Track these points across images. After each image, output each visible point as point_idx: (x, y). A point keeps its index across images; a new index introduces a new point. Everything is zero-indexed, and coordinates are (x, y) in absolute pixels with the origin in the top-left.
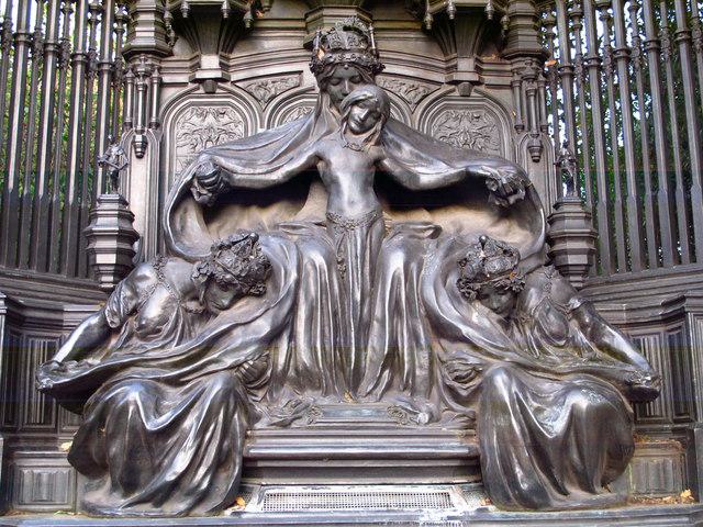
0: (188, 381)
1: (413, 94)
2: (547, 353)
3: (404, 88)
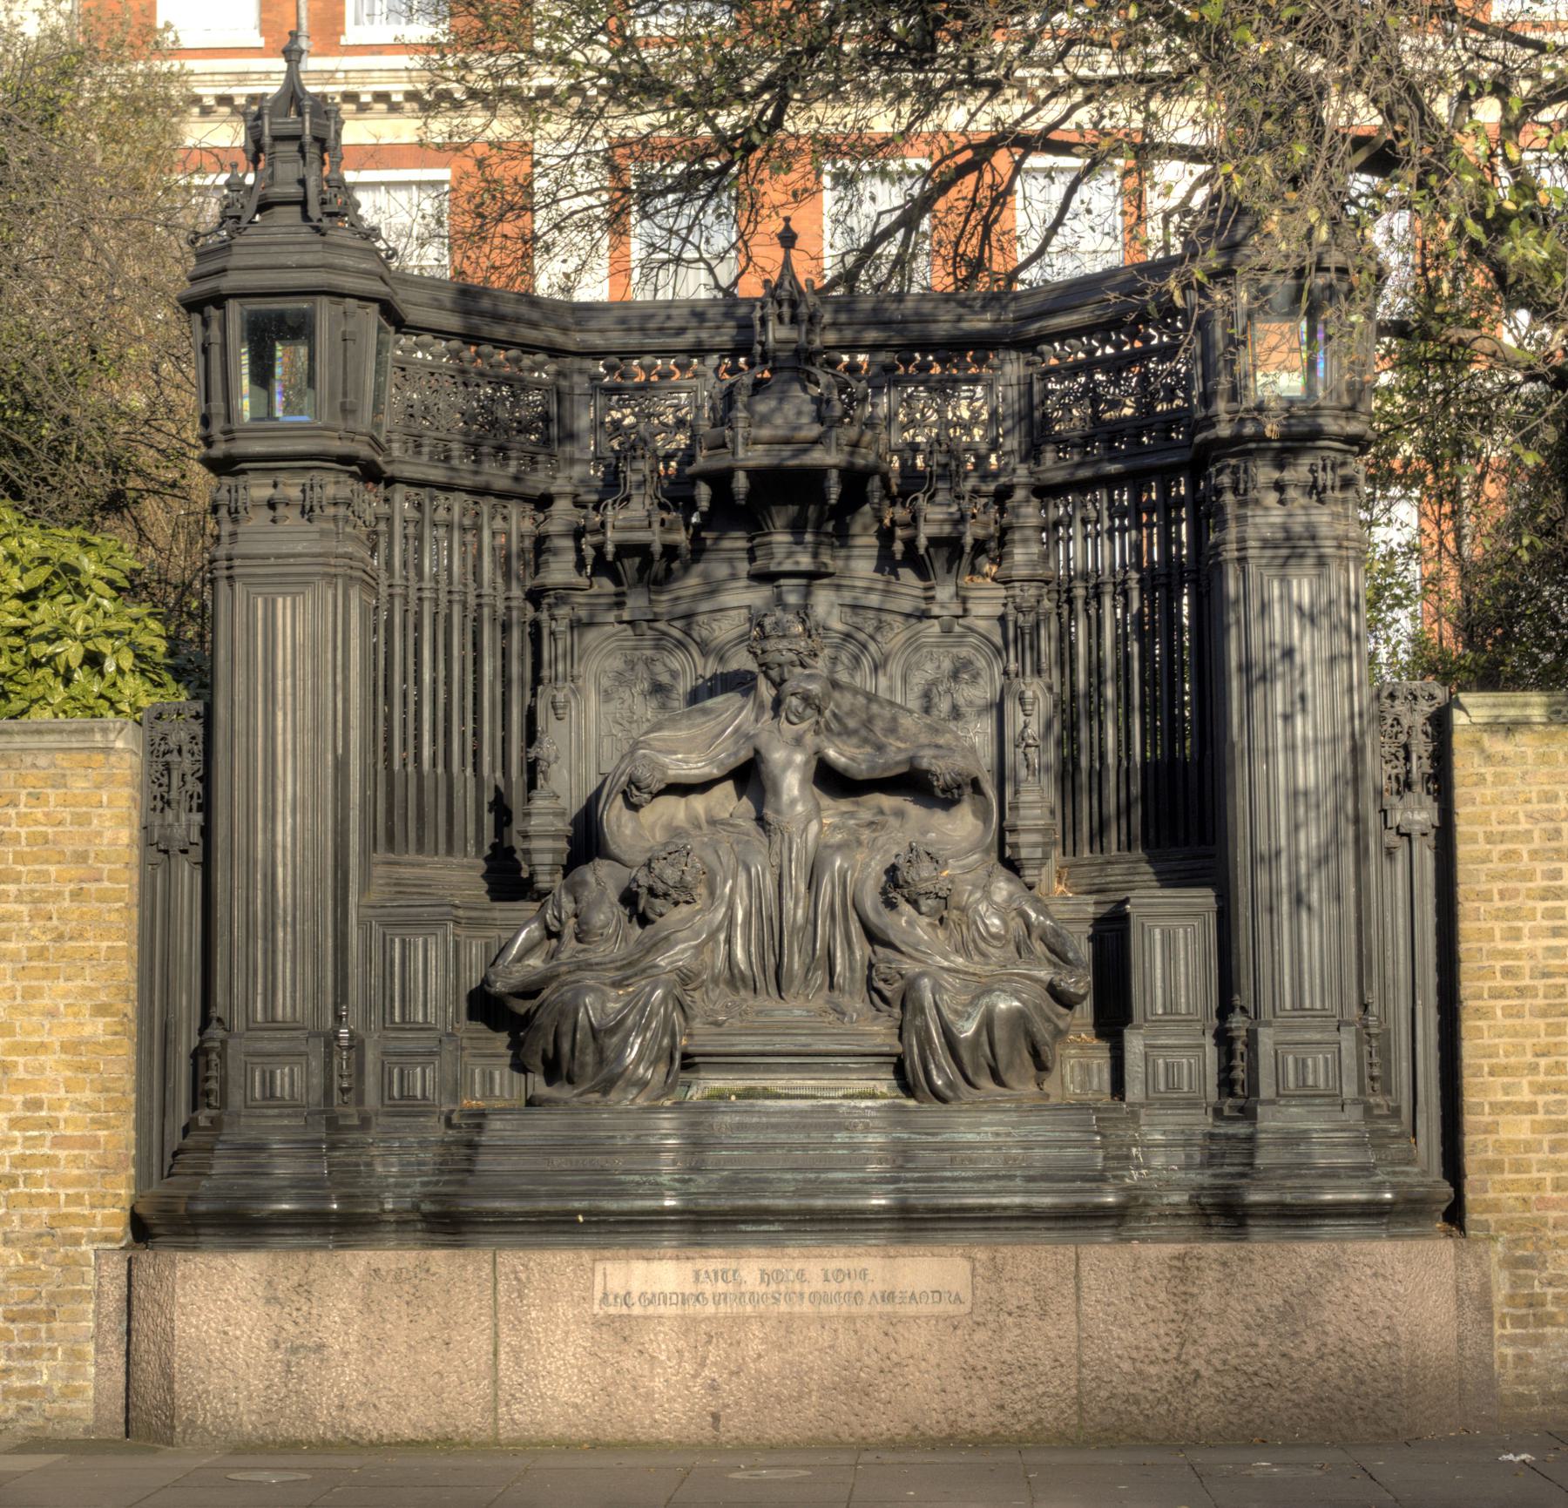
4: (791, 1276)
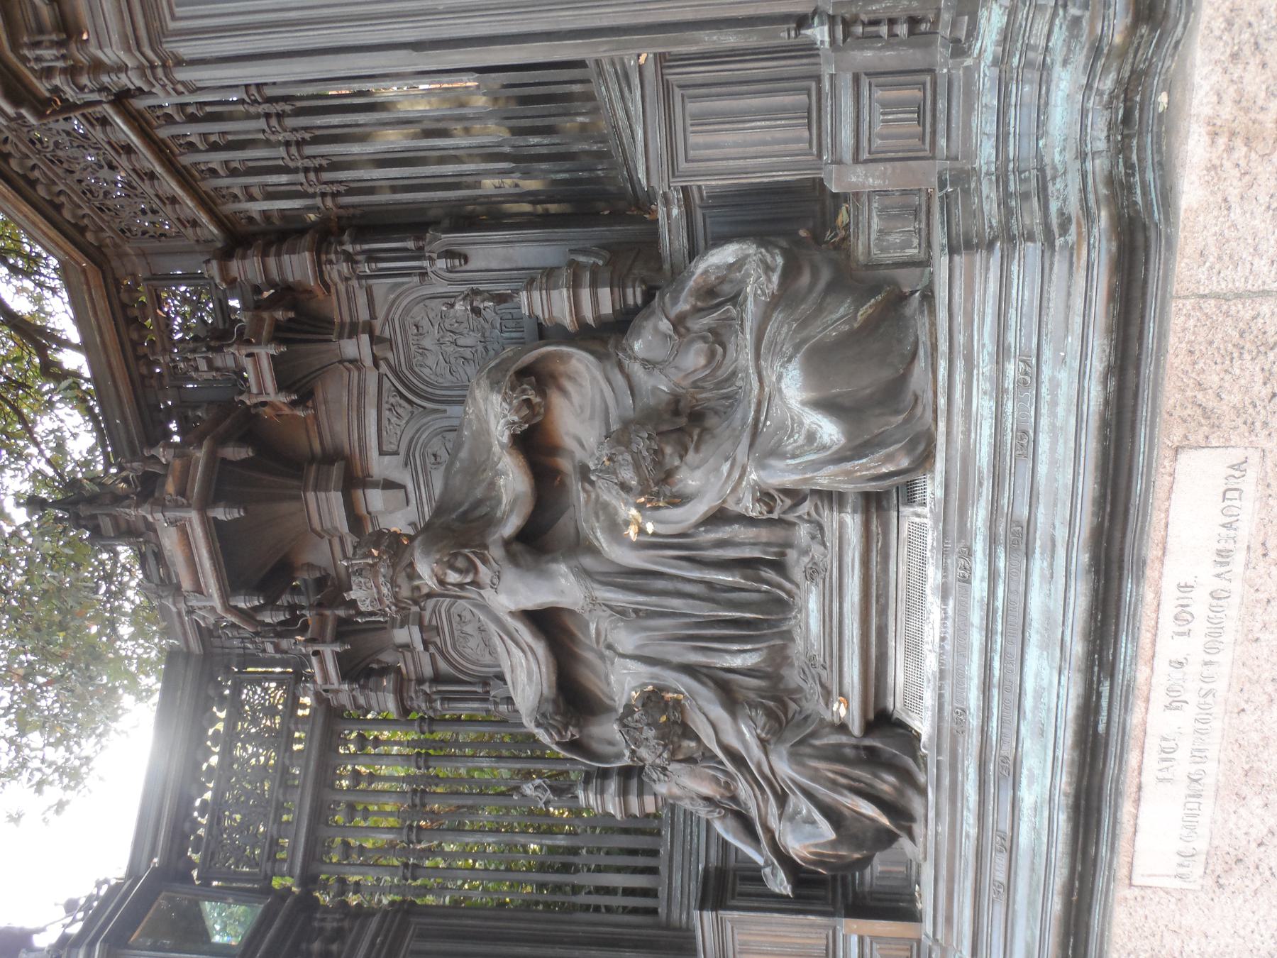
0: (782, 789)
1: (400, 410)
2: (734, 374)
3: (394, 420)
4: (1177, 674)
